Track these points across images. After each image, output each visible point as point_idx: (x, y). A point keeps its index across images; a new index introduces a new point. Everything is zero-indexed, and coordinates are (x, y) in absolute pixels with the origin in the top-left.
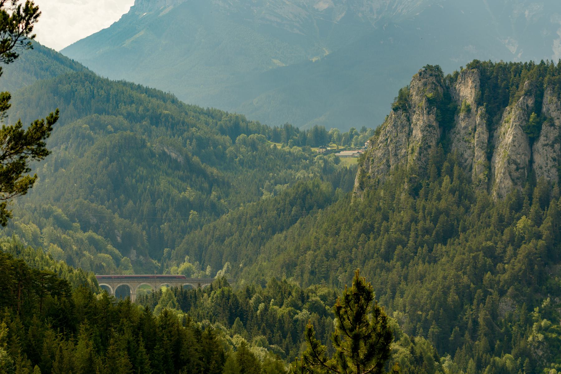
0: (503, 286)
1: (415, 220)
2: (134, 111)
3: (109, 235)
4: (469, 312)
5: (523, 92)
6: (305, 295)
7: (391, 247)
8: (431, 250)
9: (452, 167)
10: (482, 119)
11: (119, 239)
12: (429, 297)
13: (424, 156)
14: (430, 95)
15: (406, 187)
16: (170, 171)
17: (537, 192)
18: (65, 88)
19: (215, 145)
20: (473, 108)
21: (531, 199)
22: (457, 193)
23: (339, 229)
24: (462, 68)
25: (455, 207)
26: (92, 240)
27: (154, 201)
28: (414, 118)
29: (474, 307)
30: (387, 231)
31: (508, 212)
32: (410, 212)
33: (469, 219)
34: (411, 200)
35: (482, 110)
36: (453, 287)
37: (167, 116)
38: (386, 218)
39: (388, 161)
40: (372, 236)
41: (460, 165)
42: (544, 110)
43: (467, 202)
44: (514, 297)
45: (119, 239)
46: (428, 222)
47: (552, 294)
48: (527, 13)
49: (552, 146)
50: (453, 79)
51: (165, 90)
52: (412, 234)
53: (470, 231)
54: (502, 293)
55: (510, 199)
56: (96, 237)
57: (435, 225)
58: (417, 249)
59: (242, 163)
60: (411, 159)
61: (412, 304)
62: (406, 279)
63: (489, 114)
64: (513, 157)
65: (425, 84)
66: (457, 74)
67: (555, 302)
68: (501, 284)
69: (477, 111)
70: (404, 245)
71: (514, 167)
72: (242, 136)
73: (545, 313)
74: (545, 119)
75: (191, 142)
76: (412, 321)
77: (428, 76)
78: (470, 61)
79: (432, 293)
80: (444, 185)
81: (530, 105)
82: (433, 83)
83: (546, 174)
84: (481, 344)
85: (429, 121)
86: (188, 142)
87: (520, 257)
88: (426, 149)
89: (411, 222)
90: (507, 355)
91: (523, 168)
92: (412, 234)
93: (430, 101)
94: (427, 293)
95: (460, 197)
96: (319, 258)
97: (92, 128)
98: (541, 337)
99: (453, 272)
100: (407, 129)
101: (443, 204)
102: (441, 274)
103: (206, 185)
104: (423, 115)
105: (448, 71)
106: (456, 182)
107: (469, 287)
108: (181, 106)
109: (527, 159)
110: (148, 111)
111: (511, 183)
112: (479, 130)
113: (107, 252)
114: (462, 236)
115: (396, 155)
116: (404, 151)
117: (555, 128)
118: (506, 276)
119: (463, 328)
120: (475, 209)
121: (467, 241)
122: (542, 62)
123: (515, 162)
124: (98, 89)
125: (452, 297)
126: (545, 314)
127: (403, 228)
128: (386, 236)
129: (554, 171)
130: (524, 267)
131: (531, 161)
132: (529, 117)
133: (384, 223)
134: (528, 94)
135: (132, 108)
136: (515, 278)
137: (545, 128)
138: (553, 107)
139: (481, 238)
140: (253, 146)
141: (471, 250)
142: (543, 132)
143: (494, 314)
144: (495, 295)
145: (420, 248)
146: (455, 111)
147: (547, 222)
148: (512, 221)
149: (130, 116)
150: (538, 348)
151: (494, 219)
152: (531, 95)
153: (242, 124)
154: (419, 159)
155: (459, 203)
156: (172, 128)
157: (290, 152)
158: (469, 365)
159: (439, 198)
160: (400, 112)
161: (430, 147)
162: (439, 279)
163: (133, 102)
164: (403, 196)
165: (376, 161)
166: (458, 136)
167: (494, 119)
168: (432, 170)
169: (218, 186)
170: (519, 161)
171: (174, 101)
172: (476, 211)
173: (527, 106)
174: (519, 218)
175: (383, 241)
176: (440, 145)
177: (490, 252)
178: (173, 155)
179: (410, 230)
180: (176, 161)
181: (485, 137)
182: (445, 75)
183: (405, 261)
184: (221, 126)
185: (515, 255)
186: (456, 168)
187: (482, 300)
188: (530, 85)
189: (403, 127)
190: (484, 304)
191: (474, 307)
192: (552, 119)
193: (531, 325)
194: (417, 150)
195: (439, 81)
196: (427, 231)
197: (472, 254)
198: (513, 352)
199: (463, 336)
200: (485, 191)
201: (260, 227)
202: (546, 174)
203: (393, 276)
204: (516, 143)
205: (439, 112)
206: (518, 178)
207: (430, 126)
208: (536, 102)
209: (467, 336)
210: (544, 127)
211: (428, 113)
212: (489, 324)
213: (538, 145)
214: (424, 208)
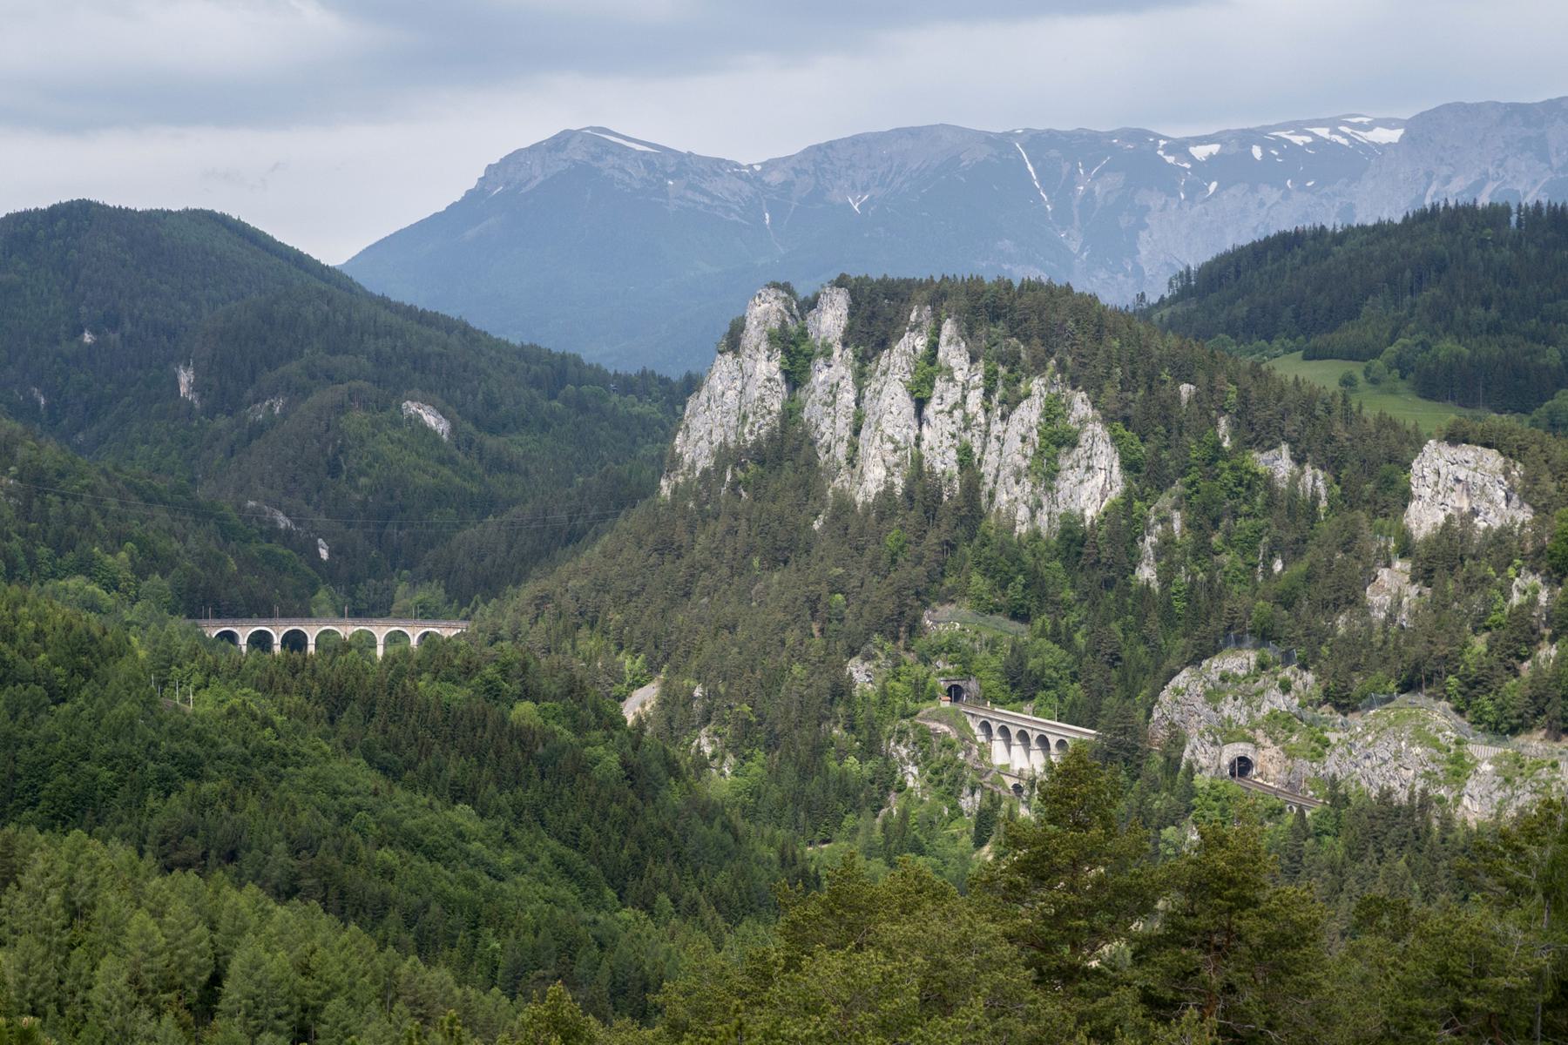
1: (733, 532)
11: (324, 554)
28: (748, 364)
35: (849, 353)
42: (941, 355)
45: (324, 554)
48: (1097, 189)
71: (890, 446)
77: (771, 299)
81: (918, 348)
82: (779, 310)
83: (939, 458)
100: (738, 384)
111: (884, 473)
123: (891, 439)
131: (919, 439)
137: (939, 385)
142: (936, 393)
161: (770, 413)
164: (724, 490)
170: (897, 437)
171: (466, 330)
173: (914, 349)
181: (847, 397)
192: (950, 370)
202: (939, 458)
206: (897, 465)
210: (937, 383)
213: (929, 411)
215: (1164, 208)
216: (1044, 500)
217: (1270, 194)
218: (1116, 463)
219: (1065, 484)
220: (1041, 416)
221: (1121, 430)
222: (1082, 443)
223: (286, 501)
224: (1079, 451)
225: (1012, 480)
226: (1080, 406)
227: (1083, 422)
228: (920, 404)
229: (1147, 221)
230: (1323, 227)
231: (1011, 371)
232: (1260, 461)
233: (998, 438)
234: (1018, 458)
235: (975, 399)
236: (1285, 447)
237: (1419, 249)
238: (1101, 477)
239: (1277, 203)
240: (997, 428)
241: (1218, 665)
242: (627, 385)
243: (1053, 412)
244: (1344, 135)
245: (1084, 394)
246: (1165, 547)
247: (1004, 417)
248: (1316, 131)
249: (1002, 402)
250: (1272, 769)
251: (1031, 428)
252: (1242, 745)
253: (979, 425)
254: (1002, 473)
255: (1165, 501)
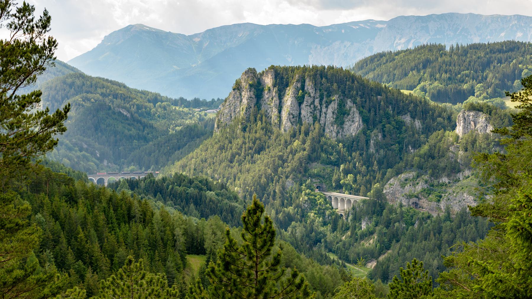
0: (288, 174)
1: (244, 143)
2: (105, 92)
3: (93, 154)
4: (271, 187)
5: (295, 80)
6: (192, 181)
7: (233, 156)
8: (252, 157)
9: (262, 117)
10: (276, 94)
11: (98, 155)
12: (252, 180)
13: (248, 112)
14: (251, 82)
15: (240, 127)
16: (123, 121)
17: (303, 128)
18: (69, 81)
19: (146, 108)
20: (272, 88)
21: (300, 132)
22: (265, 129)
23: (208, 148)
24: (266, 69)
25: (264, 136)
26: (84, 156)
27: (115, 136)
28: (243, 93)
29: (274, 184)
30: (231, 148)
31: (289, 138)
32: (242, 139)
33: (271, 142)
34: (242, 133)
35: (276, 89)
36: (264, 175)
37: (121, 94)
38: (231, 142)
39: (231, 115)
40: (224, 151)
41: (266, 116)
42: (306, 89)
43: (269, 134)
44: (293, 179)
45: (98, 155)
46: (251, 143)
47: (311, 177)
48: (296, 42)
49: (310, 106)
50: (262, 74)
51: (120, 81)
52: (243, 150)
53: (271, 147)
54: (287, 177)
55: (290, 132)
56: (87, 154)
57: (254, 145)
58: (245, 157)
59: (159, 117)
60: (242, 113)
61: (244, 184)
62: (240, 171)
63: (279, 91)
64: (291, 112)
65: (248, 77)
66: (263, 72)
67: (313, 181)
68: (287, 173)
69: (273, 90)
70: (240, 155)
71: (292, 116)
72: (159, 103)
73: (308, 186)
74: (306, 93)
75: (134, 106)
76: (244, 192)
78: (270, 66)
79: (253, 178)
80: (258, 125)
84: (277, 202)
85: (250, 95)
86: (132, 106)
87: (295, 159)
88: (249, 109)
89: (243, 144)
90: (290, 207)
91: (296, 117)
92: (243, 150)
93: (251, 86)
94: (251, 178)
95: (266, 132)
96: (198, 162)
97: (84, 101)
98: (306, 198)
99: (263, 168)
100: (240, 99)
101: (258, 135)
102: (257, 169)
103: (141, 128)
104: (247, 92)
105: (259, 71)
106: (264, 124)
107: (271, 174)
108: (128, 89)
109: (298, 113)
110: (112, 91)
111: (290, 124)
112: (275, 99)
113: (92, 161)
114: (267, 150)
115: (235, 112)
116: (238, 109)
117: (311, 98)
118: (289, 169)
119: (269, 195)
120: (273, 137)
121: (270, 153)
122: (304, 66)
123: (292, 114)
124: (86, 81)
125: (263, 180)
126: (309, 187)
127: (239, 147)
128: (231, 151)
129: (311, 118)
130: (297, 165)
131: (300, 114)
132: (298, 93)
133: (230, 145)
134: (298, 81)
135: (104, 90)
136: (293, 170)
138: (310, 87)
139: (276, 151)
140: (165, 108)
141: (272, 157)
142: (305, 99)
143: (284, 188)
144: (284, 178)
145: (247, 156)
146: (262, 90)
147: (308, 143)
148: (291, 143)
149: (103, 94)
150: (305, 203)
151: (283, 142)
152: (299, 82)
153: (159, 98)
154: (246, 114)
155: (265, 134)
156: (124, 100)
157: (182, 111)
158: (272, 212)
159: (256, 132)
160: (236, 91)
161: (251, 107)
162: (257, 171)
163: (104, 87)
164: (238, 131)
165: (225, 115)
166: (264, 102)
167: (282, 94)
168: (252, 118)
169: (148, 128)
171: (125, 87)
172: (274, 138)
174: (294, 141)
175: (229, 154)
176: (256, 106)
177: (281, 158)
178: (125, 113)
179: (242, 148)
180: (126, 116)
181: (278, 102)
182: (258, 73)
183: (240, 163)
184: (148, 99)
185: (293, 159)
186: (264, 117)
187: (278, 181)
188: (299, 77)
189: (238, 98)
190: (279, 183)
191: (274, 184)
192: (309, 93)
193: (302, 192)
194: (245, 109)
195: (255, 76)
196: (250, 148)
197: (272, 159)
198: (293, 206)
199: (269, 198)
200: (278, 128)
201: (168, 148)
202: (307, 119)
203: (235, 170)
204: (292, 105)
205: (255, 90)
206: (294, 122)
207: (251, 97)
208: (302, 85)
209: (271, 198)
211: (250, 91)
212: (281, 193)
213: (303, 106)
214: (249, 137)
215: (316, 48)
216: (340, 131)
217: (348, 44)
218: (361, 120)
219: (346, 127)
220: (338, 105)
221: (361, 109)
222: (351, 114)
223: (85, 139)
224: (350, 116)
225: (330, 125)
226: (349, 103)
227: (350, 107)
228: (300, 104)
229: (311, 52)
230: (391, 51)
231: (328, 93)
232: (400, 118)
233: (325, 113)
234: (332, 119)
235: (317, 102)
236: (409, 114)
237: (423, 57)
238: (357, 124)
239: (349, 46)
240: (324, 110)
241: (403, 176)
242: (175, 103)
243: (341, 105)
244: (369, 26)
245: (350, 100)
246: (377, 144)
247: (327, 107)
248: (361, 25)
249: (327, 102)
250: (425, 205)
251: (335, 110)
252: (415, 199)
253: (319, 109)
254: (327, 124)
255: (375, 131)
